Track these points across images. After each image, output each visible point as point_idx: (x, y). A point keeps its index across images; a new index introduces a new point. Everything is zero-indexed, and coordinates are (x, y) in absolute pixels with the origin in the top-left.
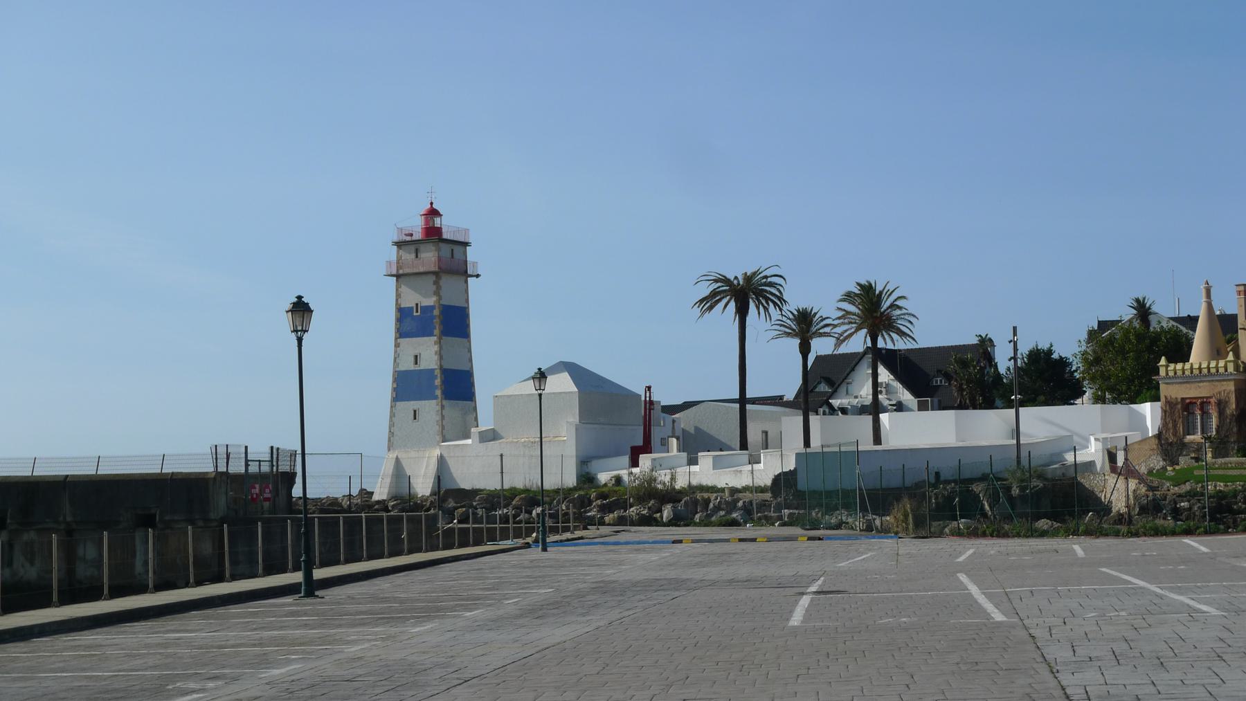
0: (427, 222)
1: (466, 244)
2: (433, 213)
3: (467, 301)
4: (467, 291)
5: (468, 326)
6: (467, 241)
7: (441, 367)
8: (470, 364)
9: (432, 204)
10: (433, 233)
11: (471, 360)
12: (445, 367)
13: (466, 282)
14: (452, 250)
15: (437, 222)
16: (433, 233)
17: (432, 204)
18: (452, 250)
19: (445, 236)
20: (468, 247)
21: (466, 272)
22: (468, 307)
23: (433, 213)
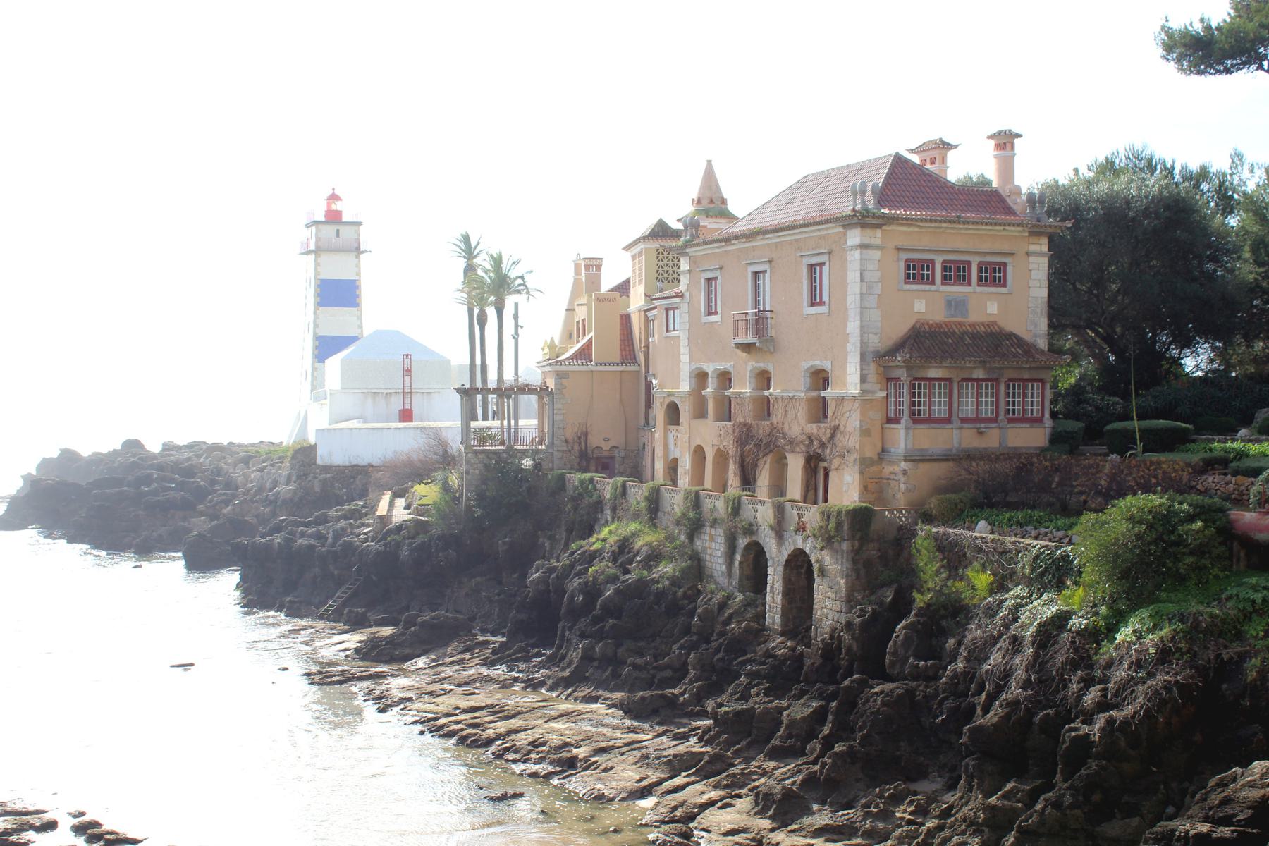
0: (329, 205)
1: (359, 224)
2: (334, 197)
3: (359, 274)
4: (358, 266)
5: (358, 296)
6: (359, 221)
7: (315, 334)
8: (360, 330)
9: (333, 189)
10: (334, 217)
11: (361, 327)
12: (320, 334)
13: (358, 257)
14: (338, 231)
15: (337, 206)
16: (334, 217)
17: (333, 189)
18: (338, 231)
19: (345, 219)
20: (361, 227)
21: (358, 248)
22: (359, 280)
23: (334, 197)
